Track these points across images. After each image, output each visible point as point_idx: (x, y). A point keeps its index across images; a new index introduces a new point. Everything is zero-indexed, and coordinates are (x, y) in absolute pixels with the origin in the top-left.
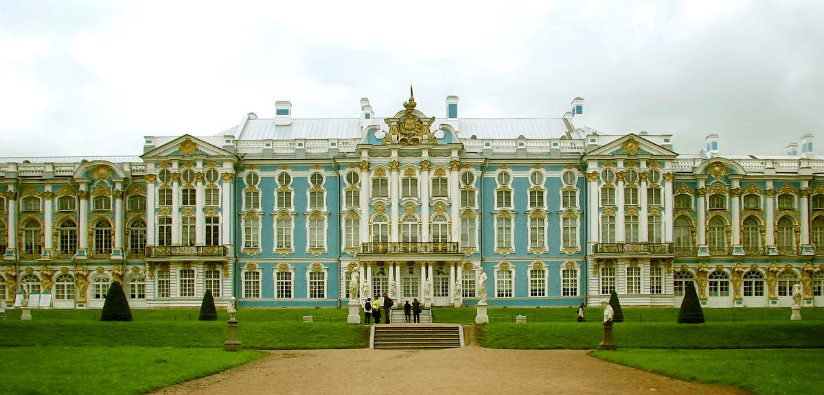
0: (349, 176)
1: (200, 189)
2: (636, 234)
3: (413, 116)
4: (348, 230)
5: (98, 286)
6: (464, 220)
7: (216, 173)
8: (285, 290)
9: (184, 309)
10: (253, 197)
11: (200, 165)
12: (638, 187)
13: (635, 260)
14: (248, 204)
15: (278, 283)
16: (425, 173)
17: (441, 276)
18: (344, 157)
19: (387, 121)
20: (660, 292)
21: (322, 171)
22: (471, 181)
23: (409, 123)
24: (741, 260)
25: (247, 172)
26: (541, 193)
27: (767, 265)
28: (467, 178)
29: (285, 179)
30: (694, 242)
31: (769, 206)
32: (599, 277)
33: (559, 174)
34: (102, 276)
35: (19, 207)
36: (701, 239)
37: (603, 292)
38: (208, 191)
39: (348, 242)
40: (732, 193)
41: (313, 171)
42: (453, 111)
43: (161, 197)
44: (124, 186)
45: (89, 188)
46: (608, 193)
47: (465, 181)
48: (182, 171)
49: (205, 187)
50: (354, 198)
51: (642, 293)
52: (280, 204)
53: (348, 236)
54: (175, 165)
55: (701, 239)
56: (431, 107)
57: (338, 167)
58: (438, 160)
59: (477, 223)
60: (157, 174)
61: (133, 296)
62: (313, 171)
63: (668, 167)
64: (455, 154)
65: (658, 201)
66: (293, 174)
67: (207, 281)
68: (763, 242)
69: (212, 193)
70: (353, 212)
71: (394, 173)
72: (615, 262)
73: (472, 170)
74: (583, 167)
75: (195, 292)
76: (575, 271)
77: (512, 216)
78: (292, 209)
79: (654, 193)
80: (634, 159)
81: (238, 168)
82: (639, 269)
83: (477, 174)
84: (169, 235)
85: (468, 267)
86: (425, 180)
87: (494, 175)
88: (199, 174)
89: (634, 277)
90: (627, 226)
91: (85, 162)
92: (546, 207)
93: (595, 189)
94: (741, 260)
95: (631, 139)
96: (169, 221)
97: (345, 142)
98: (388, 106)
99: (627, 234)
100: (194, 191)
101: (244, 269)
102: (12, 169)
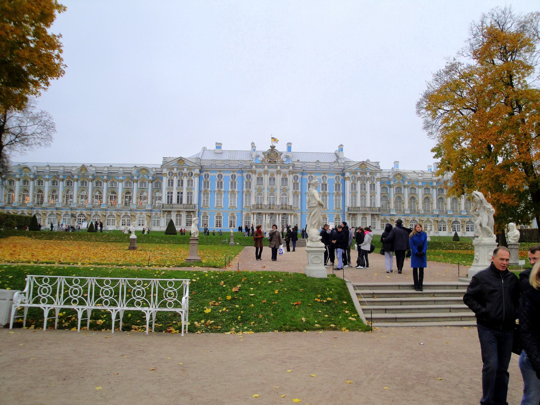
0: (247, 176)
1: (185, 180)
2: (365, 203)
4: (246, 199)
5: (140, 220)
6: (294, 196)
7: (192, 174)
10: (207, 184)
11: (185, 170)
13: (364, 214)
14: (205, 187)
16: (279, 175)
17: (284, 219)
18: (245, 168)
19: (264, 153)
21: (235, 174)
22: (297, 179)
23: (272, 155)
24: (408, 215)
25: (205, 173)
26: (326, 185)
27: (419, 218)
28: (296, 178)
29: (220, 176)
30: (389, 207)
31: (420, 192)
33: (334, 177)
36: (392, 205)
38: (188, 181)
39: (246, 204)
40: (405, 187)
41: (232, 173)
42: (289, 149)
43: (169, 183)
44: (153, 177)
47: (294, 179)
48: (178, 172)
50: (249, 185)
52: (218, 187)
53: (246, 202)
54: (175, 170)
55: (392, 205)
56: (281, 148)
57: (242, 172)
58: (284, 170)
59: (300, 197)
61: (155, 225)
62: (232, 173)
63: (378, 175)
64: (291, 168)
65: (374, 189)
66: (224, 175)
68: (418, 208)
69: (190, 182)
70: (248, 191)
71: (266, 175)
73: (298, 175)
74: (343, 175)
78: (223, 189)
79: (373, 186)
80: (365, 171)
83: (300, 176)
84: (171, 199)
85: (295, 216)
86: (278, 178)
87: (306, 177)
88: (185, 174)
90: (361, 199)
91: (135, 167)
93: (348, 183)
94: (408, 215)
95: (363, 165)
96: (172, 193)
97: (245, 161)
98: (264, 147)
99: (361, 203)
100: (182, 181)
102: (106, 169)
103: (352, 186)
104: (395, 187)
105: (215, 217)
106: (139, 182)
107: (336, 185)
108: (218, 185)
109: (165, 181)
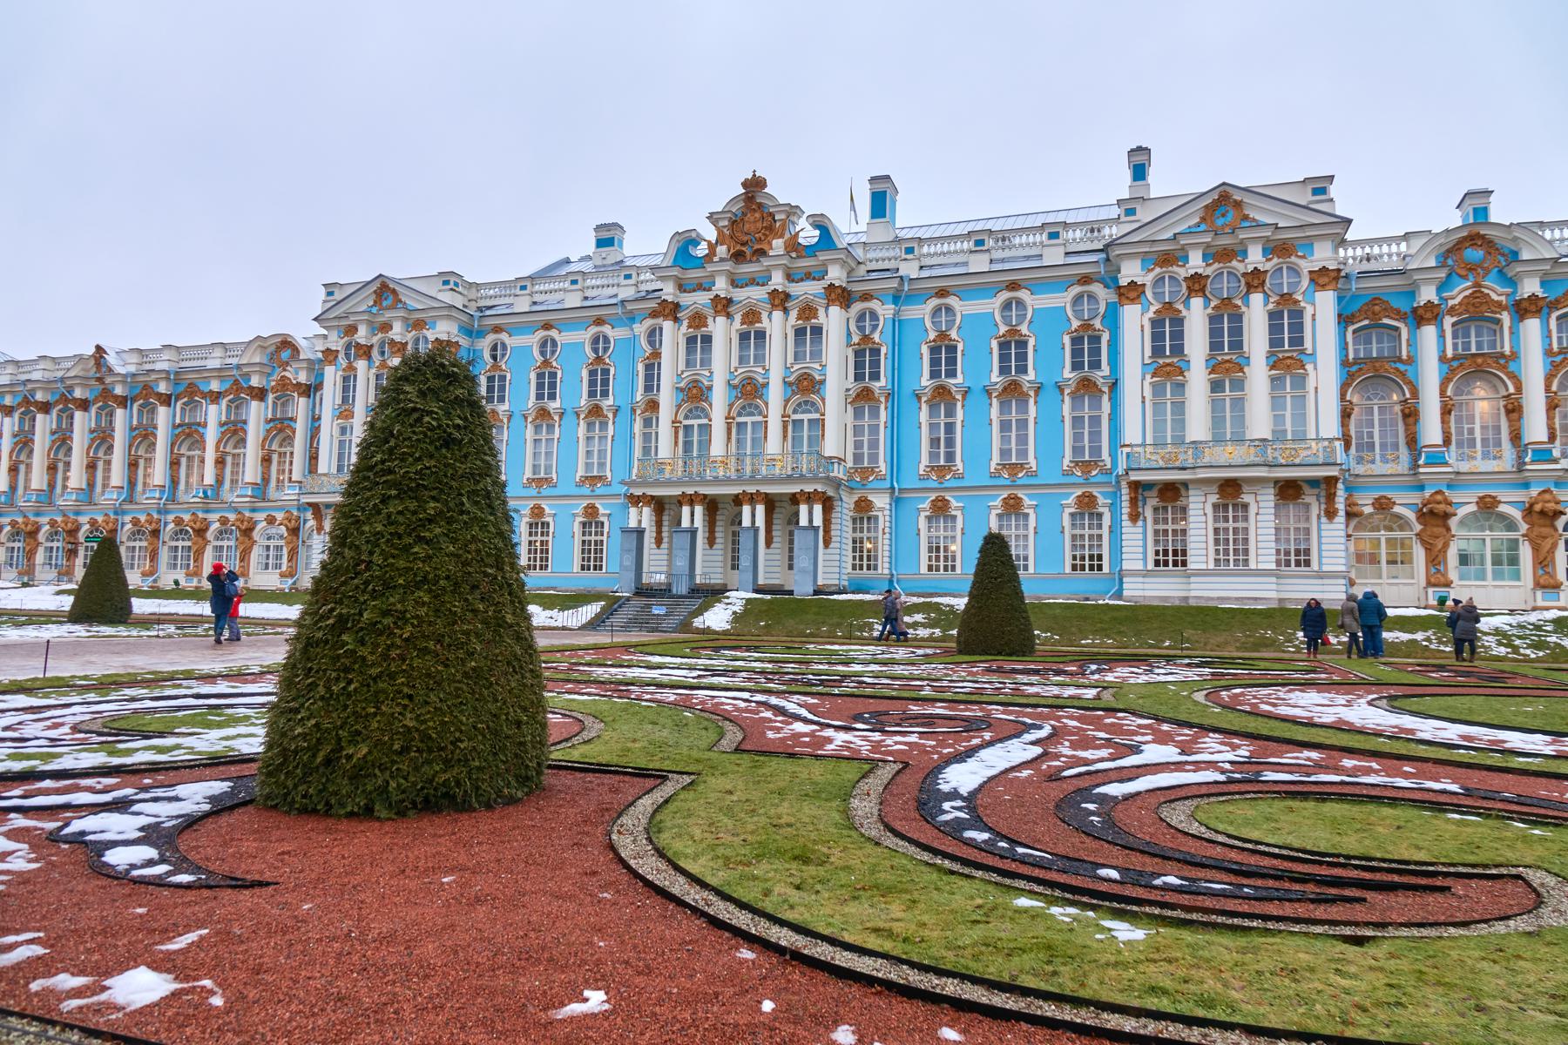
3: (760, 205)
5: (268, 548)
12: (1244, 309)
19: (713, 218)
20: (1308, 563)
23: (753, 220)
29: (547, 345)
32: (1145, 527)
37: (1157, 563)
46: (1166, 334)
47: (861, 329)
48: (375, 340)
51: (1252, 565)
63: (1323, 255)
71: (721, 320)
72: (1183, 492)
73: (874, 304)
76: (1100, 515)
77: (959, 397)
82: (1245, 506)
83: (885, 311)
86: (777, 326)
87: (922, 311)
89: (1231, 525)
92: (1031, 375)
103: (1157, 337)
104: (1448, 321)
106: (271, 397)
107: (1074, 341)
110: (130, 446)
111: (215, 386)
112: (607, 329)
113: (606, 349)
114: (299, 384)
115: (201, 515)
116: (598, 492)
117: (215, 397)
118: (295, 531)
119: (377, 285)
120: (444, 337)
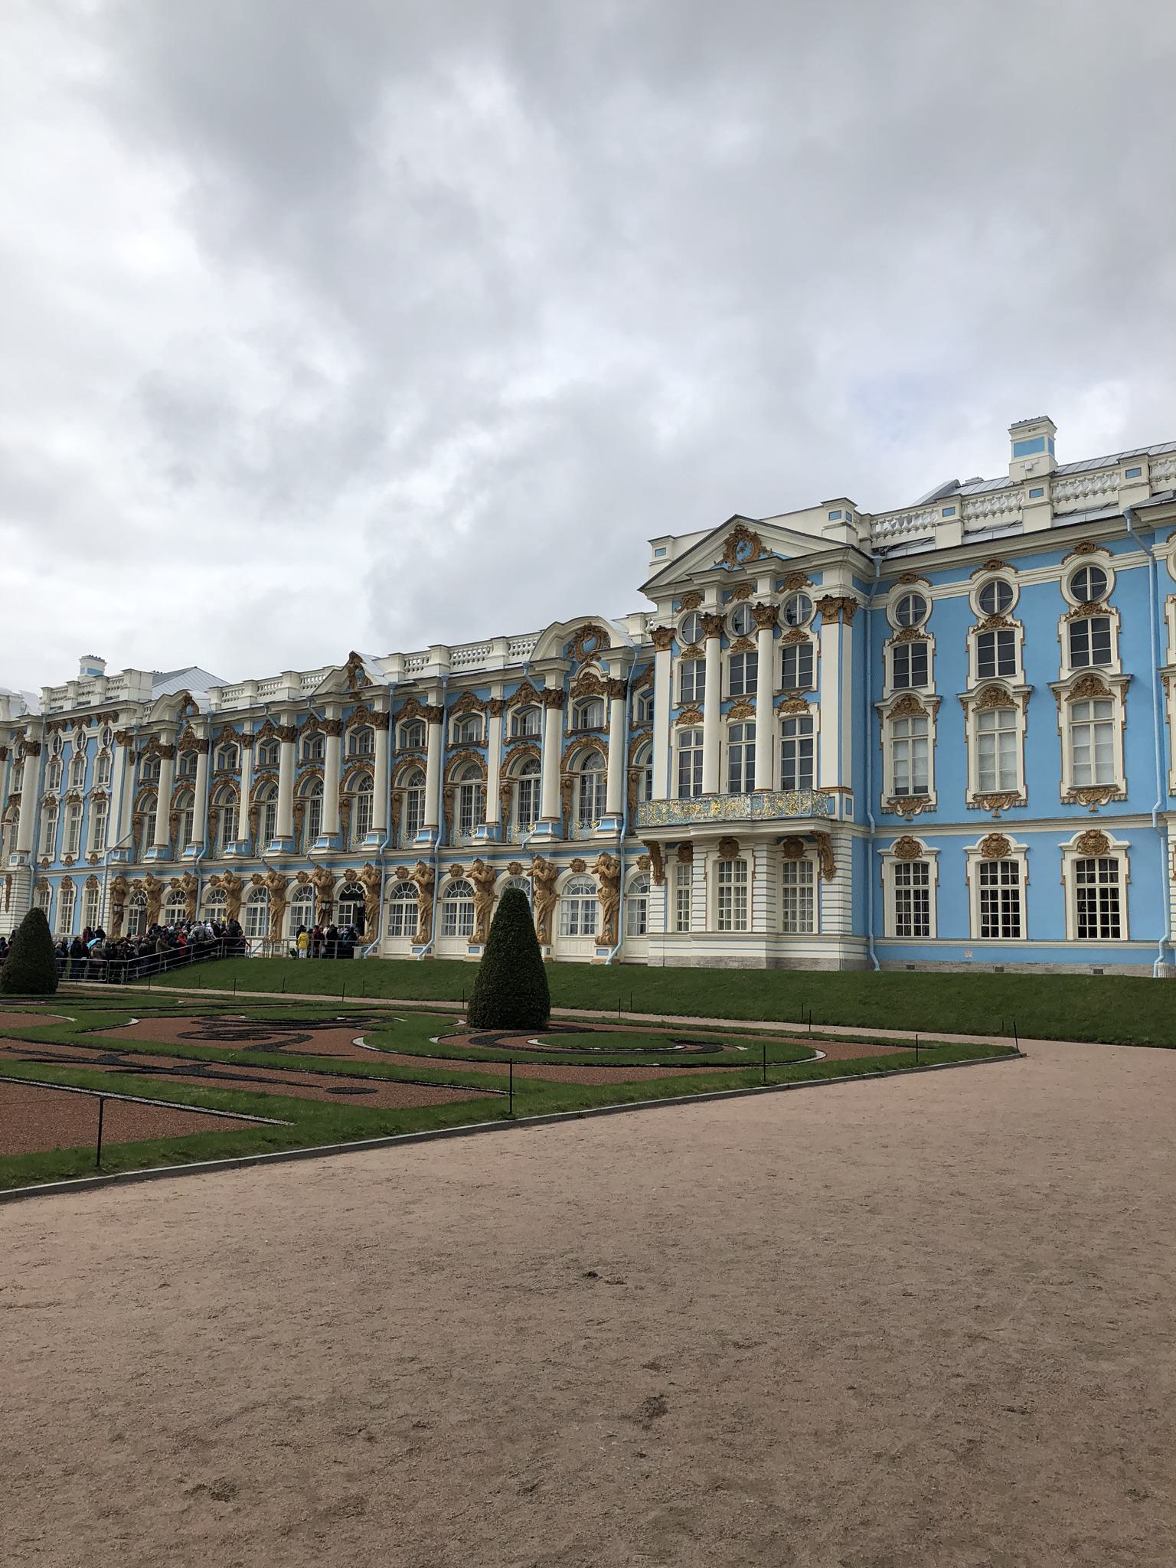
8: (1002, 914)
9: (722, 966)
14: (900, 681)
15: (984, 894)
25: (898, 591)
29: (995, 596)
34: (582, 881)
35: (447, 736)
38: (787, 653)
45: (567, 682)
48: (729, 607)
49: (780, 642)
60: (676, 626)
67: (786, 890)
69: (797, 660)
75: (748, 920)
81: (869, 585)
101: (889, 855)
105: (973, 872)
106: (571, 702)
108: (985, 655)
109: (665, 664)
110: (393, 776)
111: (496, 693)
112: (1101, 559)
113: (1099, 590)
114: (611, 682)
115: (486, 862)
116: (1104, 812)
117: (498, 708)
118: (613, 882)
119: (731, 530)
120: (835, 593)
